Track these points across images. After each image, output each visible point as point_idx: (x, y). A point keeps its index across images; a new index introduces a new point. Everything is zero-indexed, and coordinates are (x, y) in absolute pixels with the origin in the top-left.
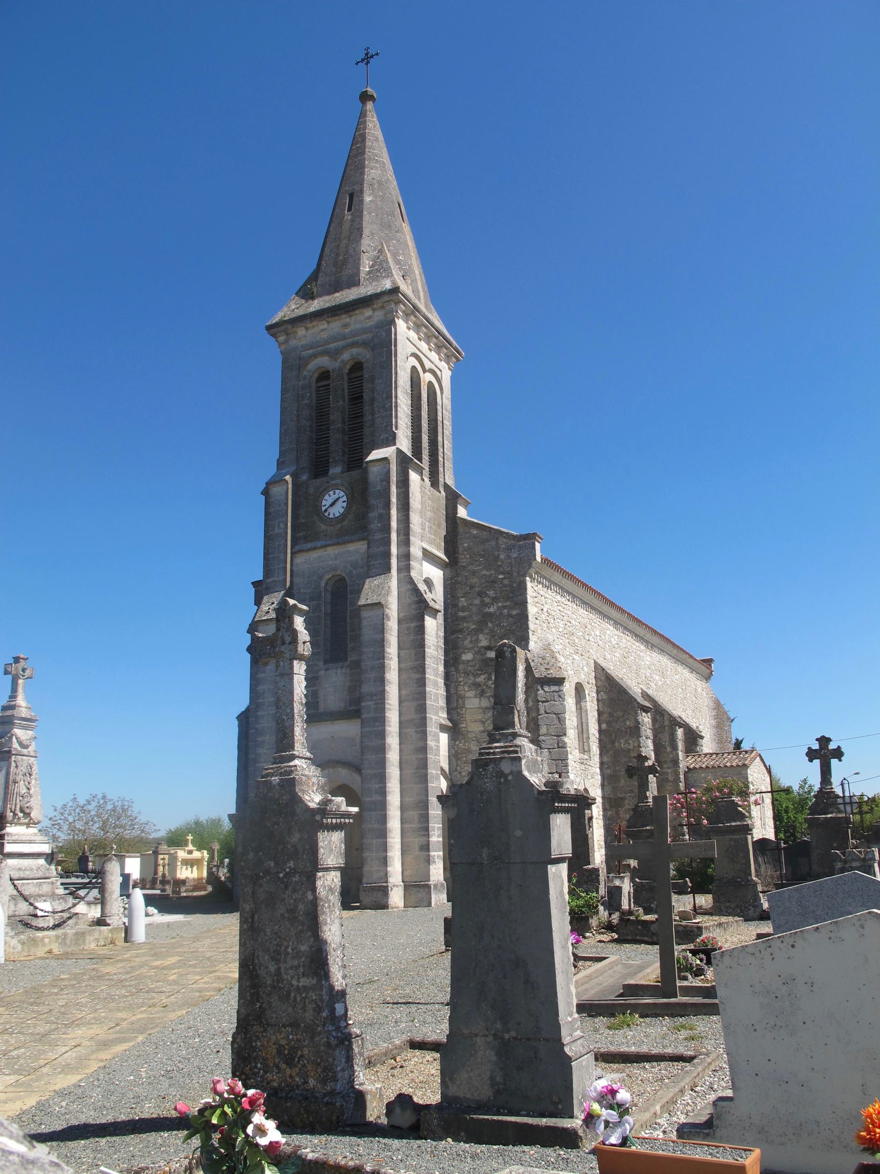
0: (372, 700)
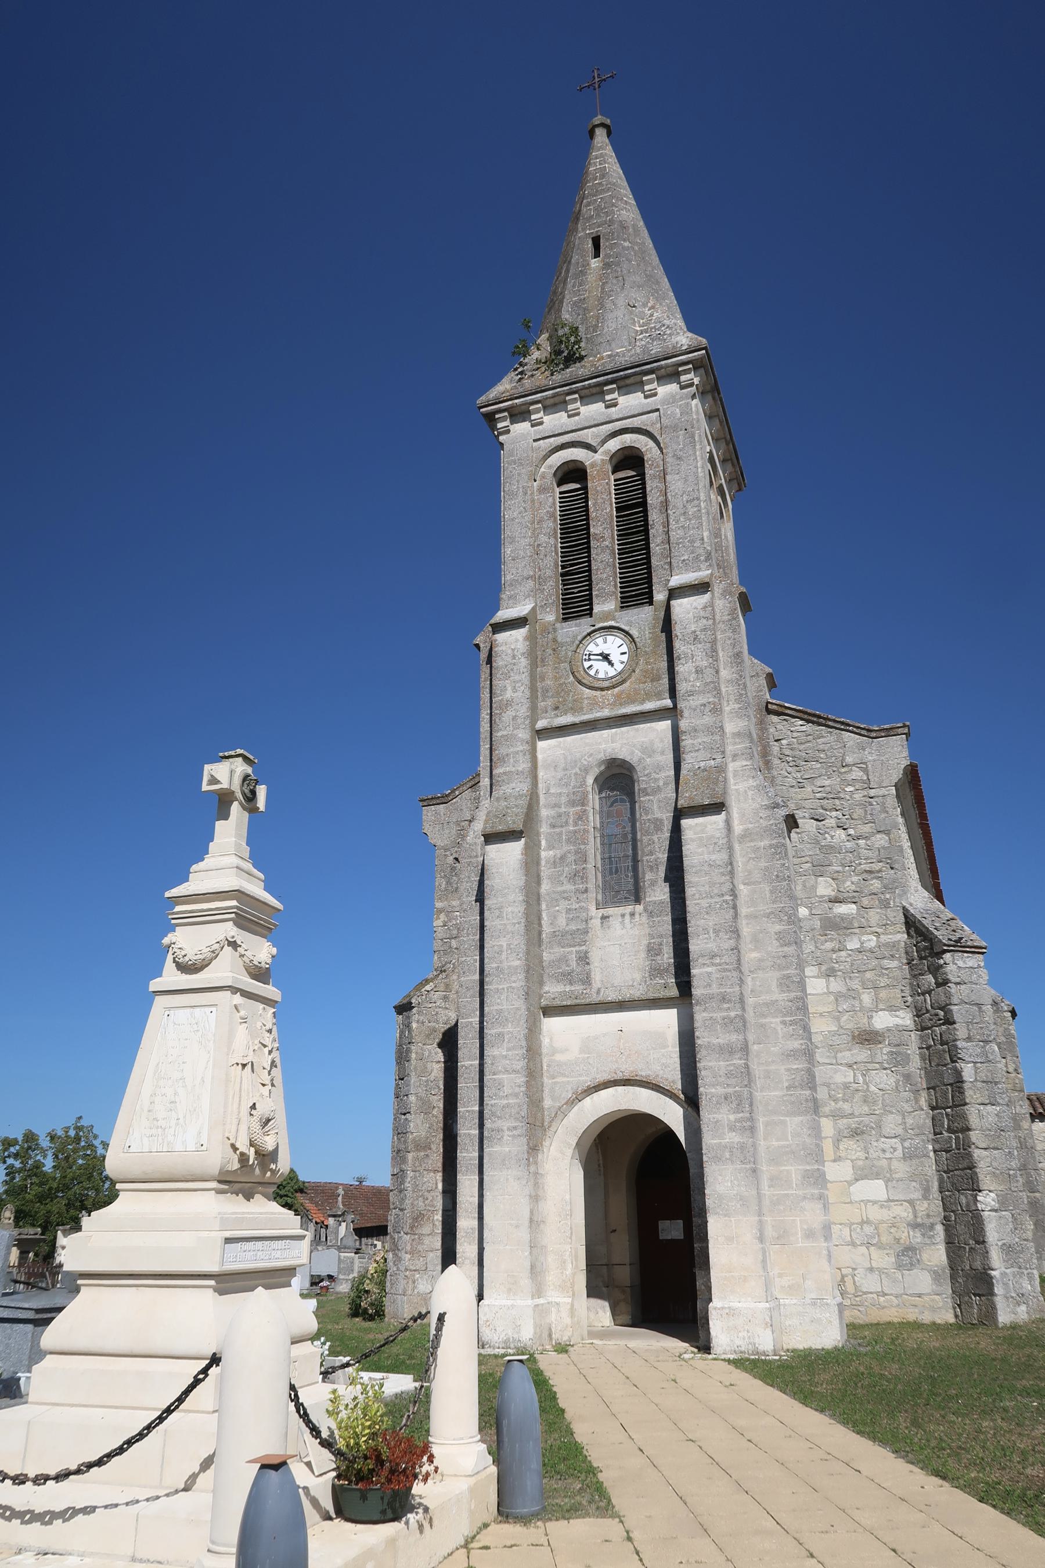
0: (713, 964)
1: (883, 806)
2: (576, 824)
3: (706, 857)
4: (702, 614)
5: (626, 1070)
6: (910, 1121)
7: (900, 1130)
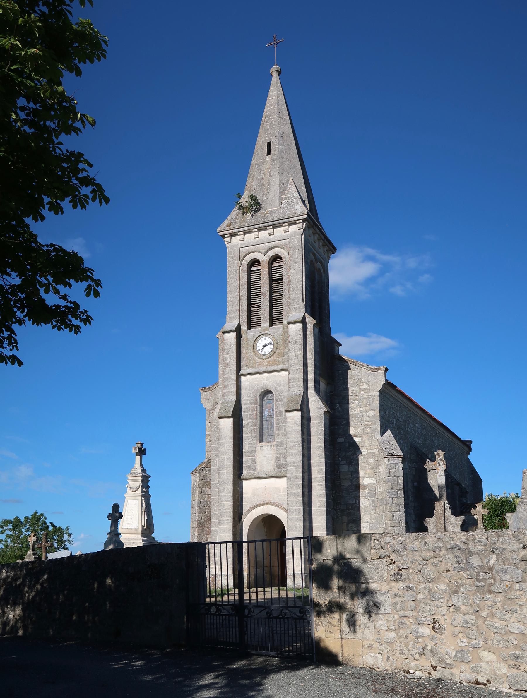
1: (373, 399)
2: (252, 412)
3: (294, 428)
4: (299, 333)
5: (267, 500)
6: (373, 517)
7: (369, 520)
